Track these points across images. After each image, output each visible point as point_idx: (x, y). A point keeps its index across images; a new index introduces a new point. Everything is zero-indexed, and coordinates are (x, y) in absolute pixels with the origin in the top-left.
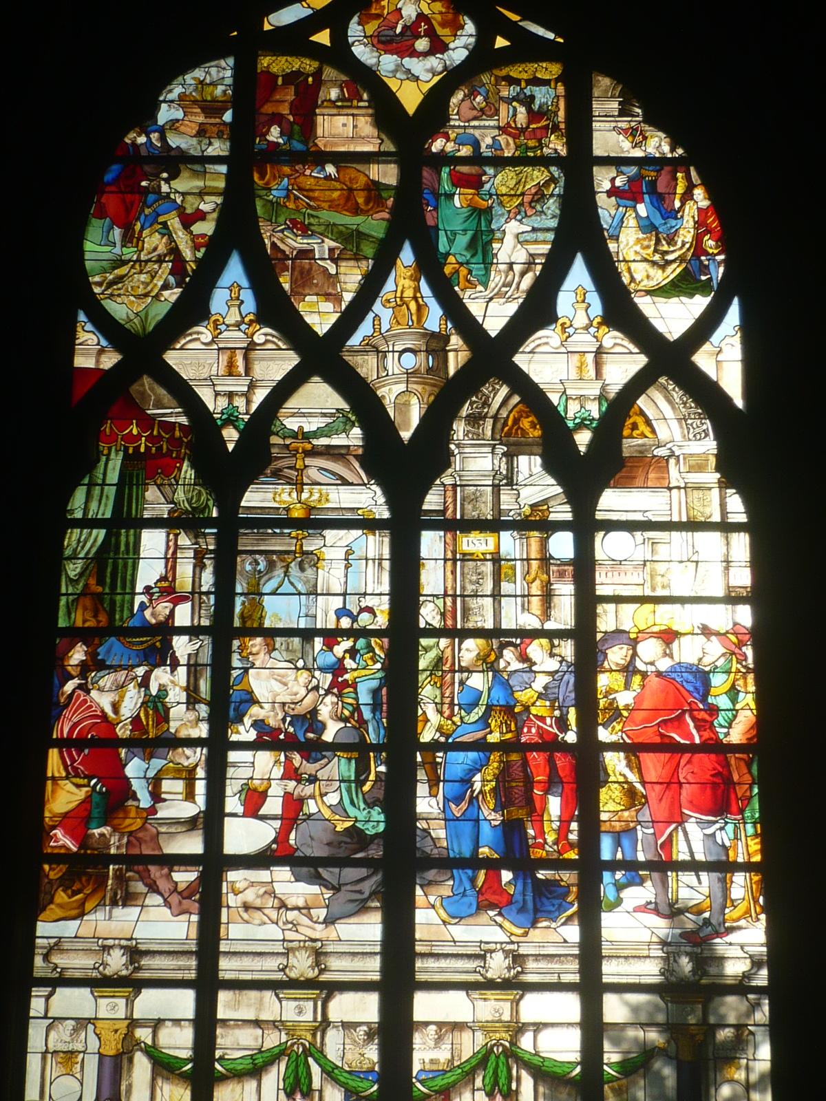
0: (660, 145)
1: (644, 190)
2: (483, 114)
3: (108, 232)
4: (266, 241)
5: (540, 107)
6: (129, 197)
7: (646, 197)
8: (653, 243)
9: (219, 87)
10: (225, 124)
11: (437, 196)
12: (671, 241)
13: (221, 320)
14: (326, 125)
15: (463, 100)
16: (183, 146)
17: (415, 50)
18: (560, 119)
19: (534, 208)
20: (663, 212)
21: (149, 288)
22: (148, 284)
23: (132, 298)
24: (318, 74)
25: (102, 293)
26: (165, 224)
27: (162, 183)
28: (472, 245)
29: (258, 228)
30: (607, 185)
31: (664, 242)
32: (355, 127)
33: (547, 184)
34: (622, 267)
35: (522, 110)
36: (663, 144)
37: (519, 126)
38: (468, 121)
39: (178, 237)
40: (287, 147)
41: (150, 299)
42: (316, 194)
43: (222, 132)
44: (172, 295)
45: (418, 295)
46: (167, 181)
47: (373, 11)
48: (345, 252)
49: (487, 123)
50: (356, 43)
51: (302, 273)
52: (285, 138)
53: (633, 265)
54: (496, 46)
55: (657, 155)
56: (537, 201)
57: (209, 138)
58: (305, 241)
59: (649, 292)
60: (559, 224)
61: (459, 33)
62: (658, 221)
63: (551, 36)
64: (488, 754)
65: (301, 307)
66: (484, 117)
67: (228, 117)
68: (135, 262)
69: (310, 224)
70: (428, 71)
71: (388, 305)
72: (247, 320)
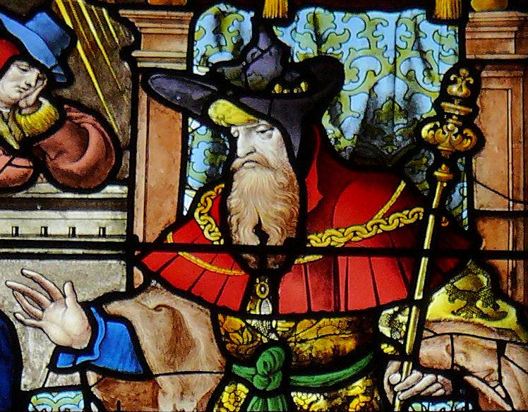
2: (41, 167)
5: (371, 125)
18: (483, 199)
37: (246, 237)
49: (58, 224)
66: (44, 188)
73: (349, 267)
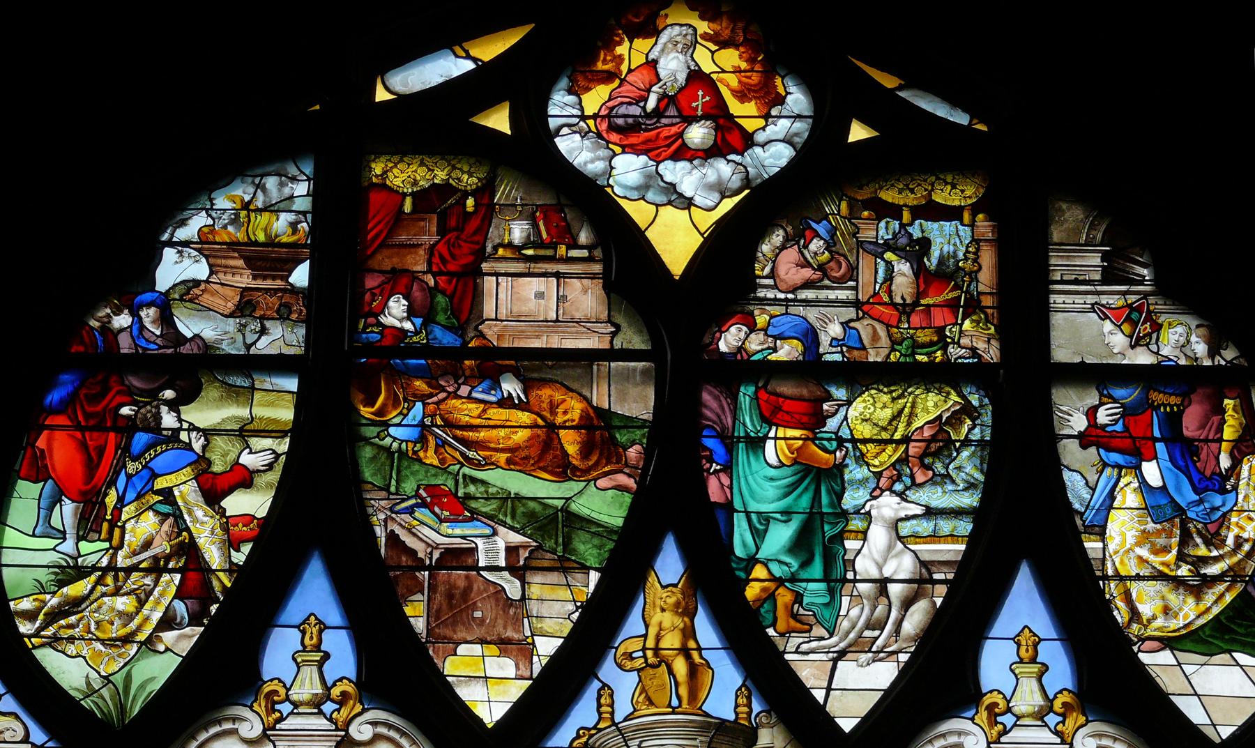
0: (1188, 341)
1: (1157, 434)
3: (51, 509)
4: (378, 531)
5: (942, 261)
6: (92, 440)
7: (1160, 447)
8: (1175, 541)
9: (283, 216)
10: (294, 290)
11: (729, 442)
12: (1213, 538)
13: (282, 692)
14: (502, 296)
15: (783, 247)
16: (209, 333)
17: (684, 145)
18: (982, 288)
19: (928, 467)
20: (1196, 478)
21: (133, 625)
22: (130, 617)
23: (98, 646)
24: (485, 192)
25: (37, 635)
26: (167, 495)
27: (164, 409)
28: (801, 545)
29: (362, 504)
30: (1079, 423)
31: (1199, 540)
32: (561, 299)
33: (956, 419)
34: (1113, 588)
35: (903, 268)
36: (1193, 338)
37: (898, 300)
38: (794, 290)
39: (196, 520)
40: (421, 339)
41: (135, 647)
42: (483, 434)
43: (287, 306)
44: (183, 640)
45: (692, 644)
46: (174, 406)
47: (600, 66)
48: (539, 554)
49: (832, 295)
50: (565, 130)
51: (450, 596)
52: (418, 321)
53: (1135, 588)
54: (851, 139)
55: (1183, 362)
56: (936, 454)
57: (262, 318)
58: (458, 532)
59: (1169, 643)
60: (982, 500)
61: (774, 112)
62: (1186, 495)
63: (962, 118)
65: (450, 667)
66: (827, 282)
67: (300, 276)
68: (105, 570)
69: (468, 497)
70: (711, 187)
71: (629, 665)
72: (336, 692)
73: (936, 312)
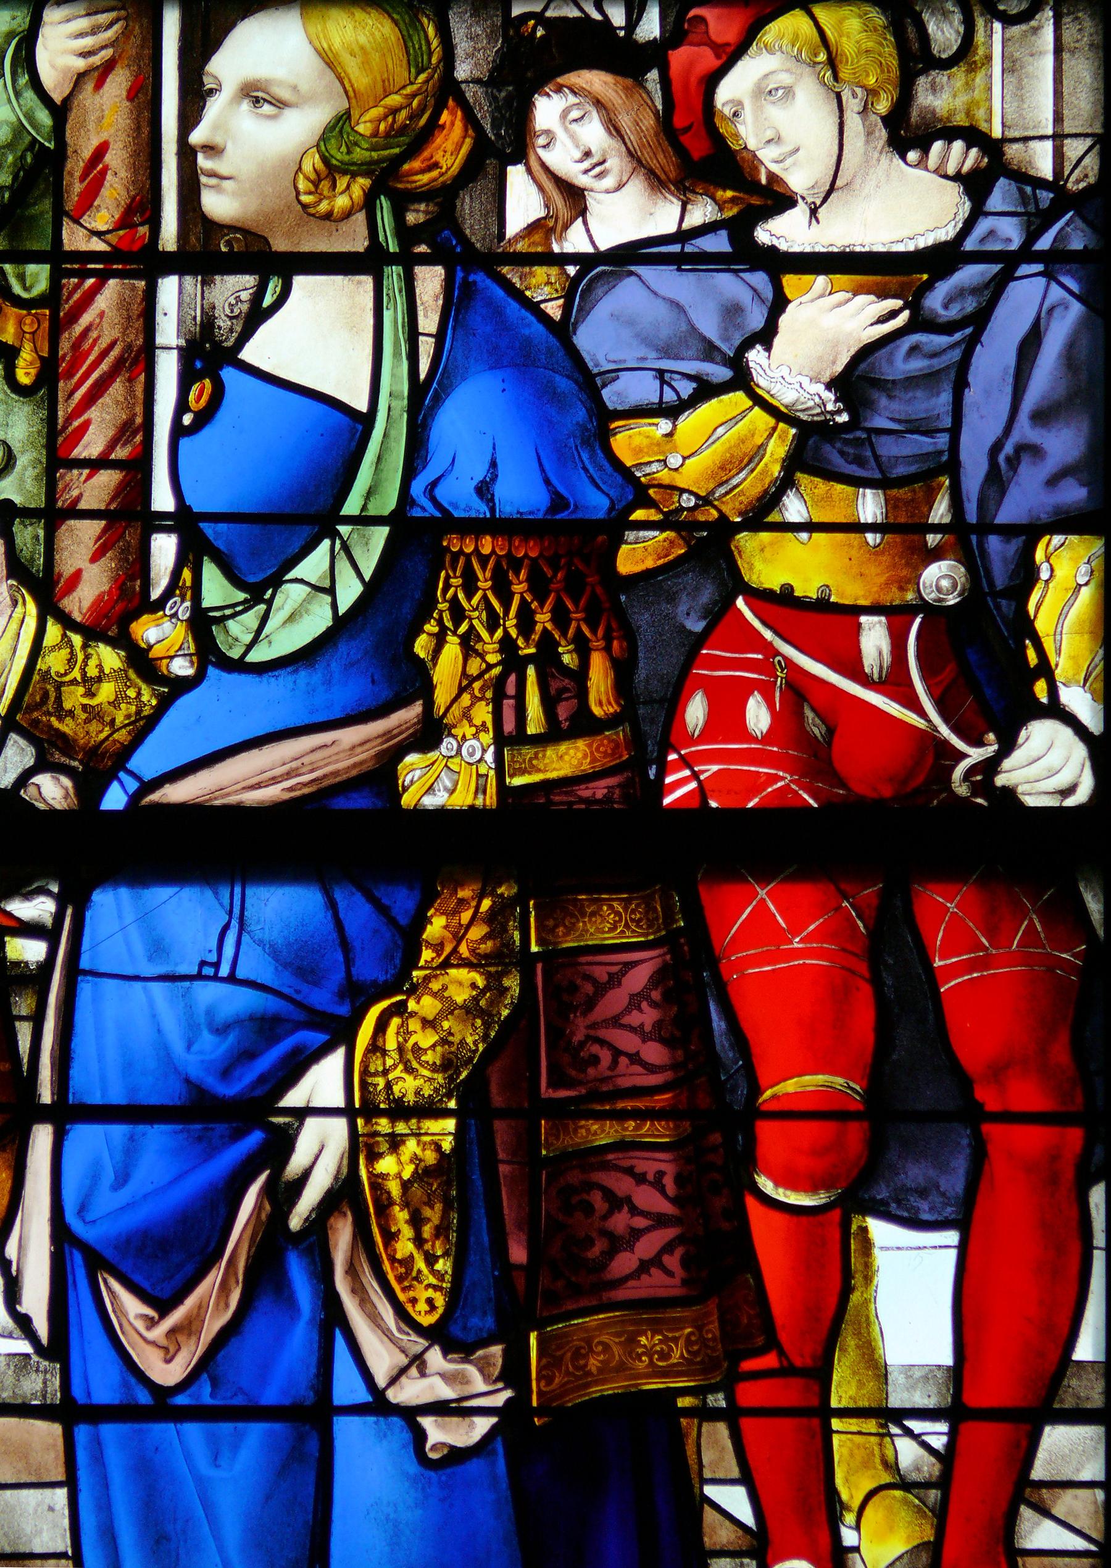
64: (402, 901)
